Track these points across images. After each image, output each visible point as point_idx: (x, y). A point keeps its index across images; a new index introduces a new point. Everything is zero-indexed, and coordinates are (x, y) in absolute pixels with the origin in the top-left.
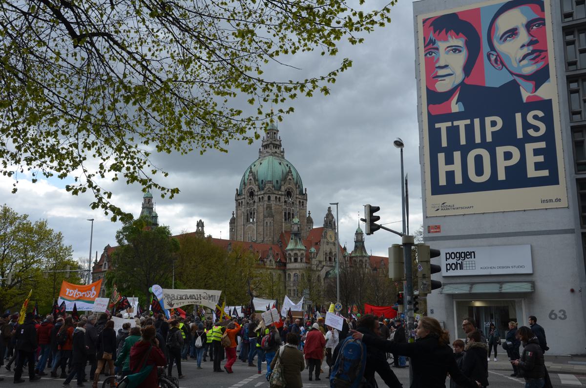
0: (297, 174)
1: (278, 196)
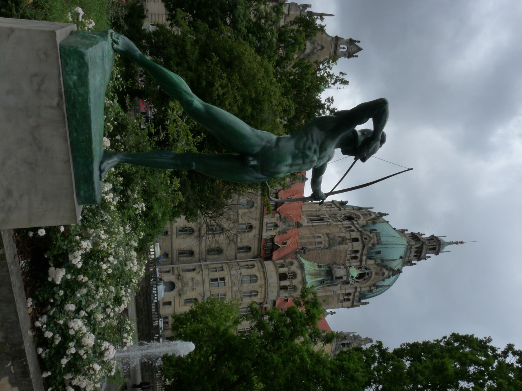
0: (389, 286)
1: (358, 255)
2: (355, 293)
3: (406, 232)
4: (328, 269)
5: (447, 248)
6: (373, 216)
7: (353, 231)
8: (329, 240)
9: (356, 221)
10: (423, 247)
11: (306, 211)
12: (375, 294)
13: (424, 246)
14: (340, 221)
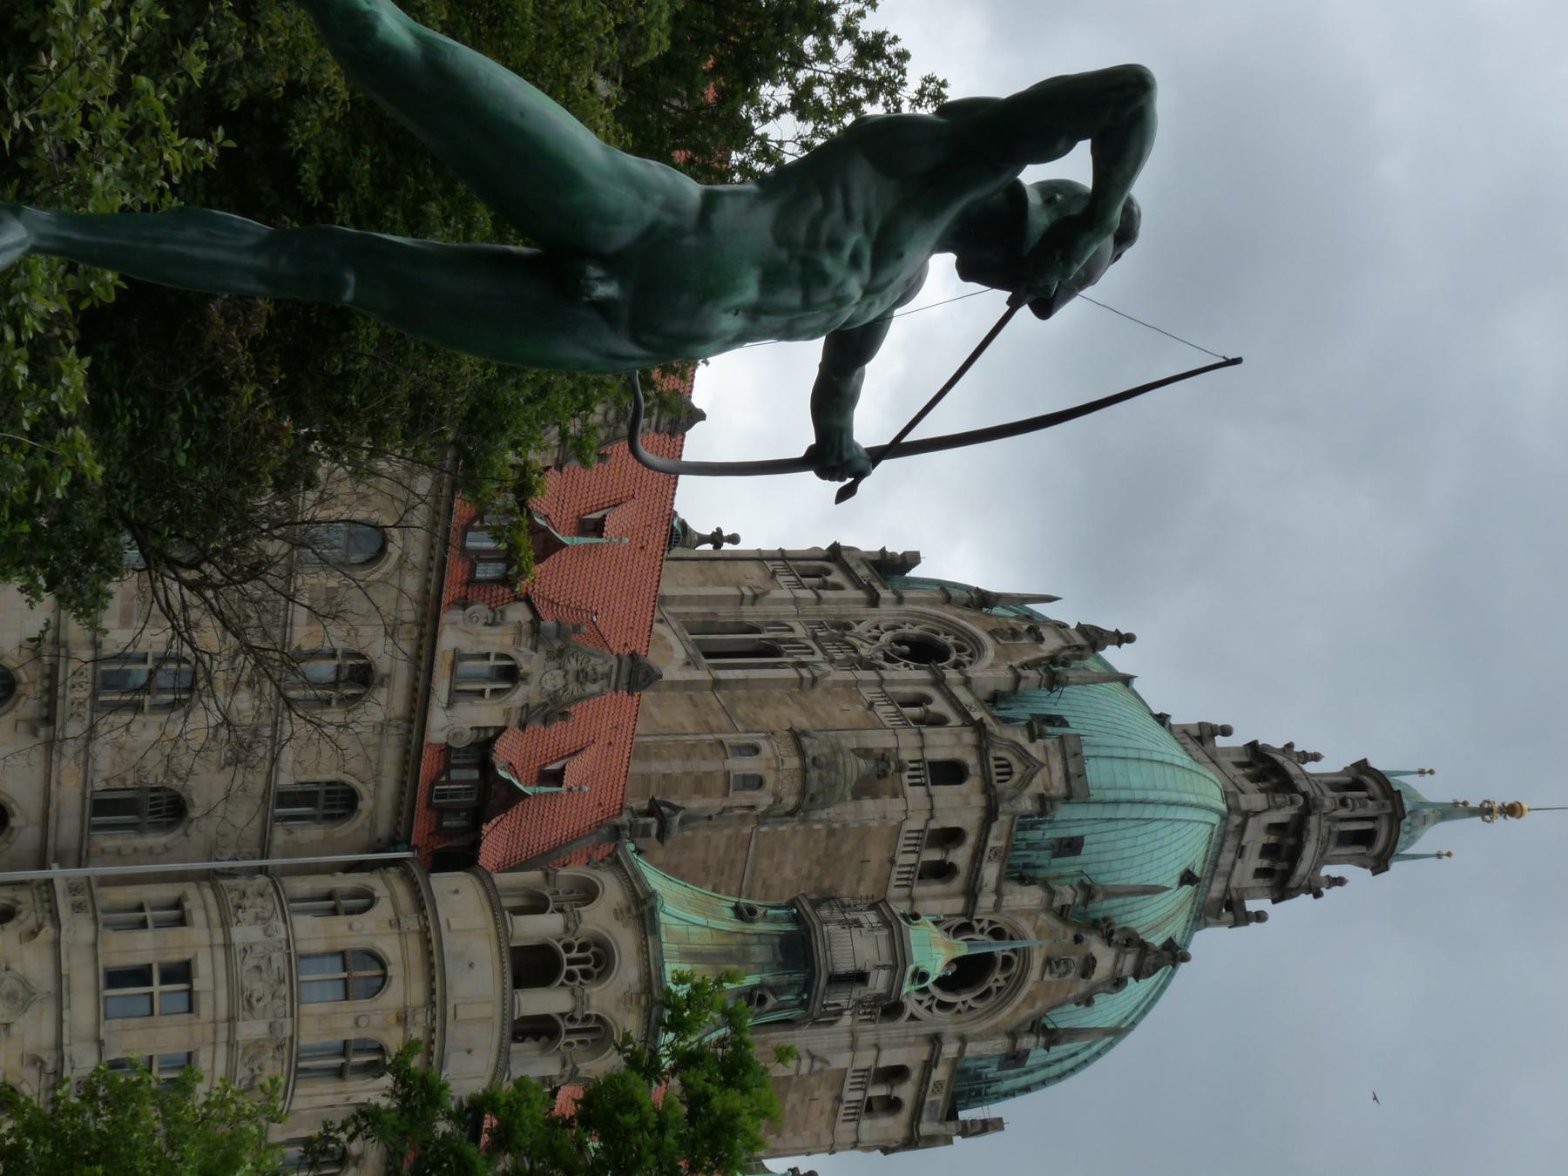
1: (960, 857)
2: (929, 1065)
3: (1220, 741)
4: (789, 927)
5: (1432, 837)
6: (1052, 643)
7: (939, 721)
8: (804, 770)
9: (957, 665)
10: (1312, 823)
11: (685, 600)
12: (1038, 1076)
13: (1313, 821)
14: (869, 665)
